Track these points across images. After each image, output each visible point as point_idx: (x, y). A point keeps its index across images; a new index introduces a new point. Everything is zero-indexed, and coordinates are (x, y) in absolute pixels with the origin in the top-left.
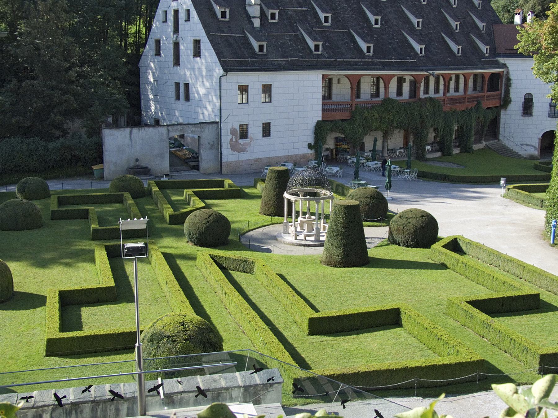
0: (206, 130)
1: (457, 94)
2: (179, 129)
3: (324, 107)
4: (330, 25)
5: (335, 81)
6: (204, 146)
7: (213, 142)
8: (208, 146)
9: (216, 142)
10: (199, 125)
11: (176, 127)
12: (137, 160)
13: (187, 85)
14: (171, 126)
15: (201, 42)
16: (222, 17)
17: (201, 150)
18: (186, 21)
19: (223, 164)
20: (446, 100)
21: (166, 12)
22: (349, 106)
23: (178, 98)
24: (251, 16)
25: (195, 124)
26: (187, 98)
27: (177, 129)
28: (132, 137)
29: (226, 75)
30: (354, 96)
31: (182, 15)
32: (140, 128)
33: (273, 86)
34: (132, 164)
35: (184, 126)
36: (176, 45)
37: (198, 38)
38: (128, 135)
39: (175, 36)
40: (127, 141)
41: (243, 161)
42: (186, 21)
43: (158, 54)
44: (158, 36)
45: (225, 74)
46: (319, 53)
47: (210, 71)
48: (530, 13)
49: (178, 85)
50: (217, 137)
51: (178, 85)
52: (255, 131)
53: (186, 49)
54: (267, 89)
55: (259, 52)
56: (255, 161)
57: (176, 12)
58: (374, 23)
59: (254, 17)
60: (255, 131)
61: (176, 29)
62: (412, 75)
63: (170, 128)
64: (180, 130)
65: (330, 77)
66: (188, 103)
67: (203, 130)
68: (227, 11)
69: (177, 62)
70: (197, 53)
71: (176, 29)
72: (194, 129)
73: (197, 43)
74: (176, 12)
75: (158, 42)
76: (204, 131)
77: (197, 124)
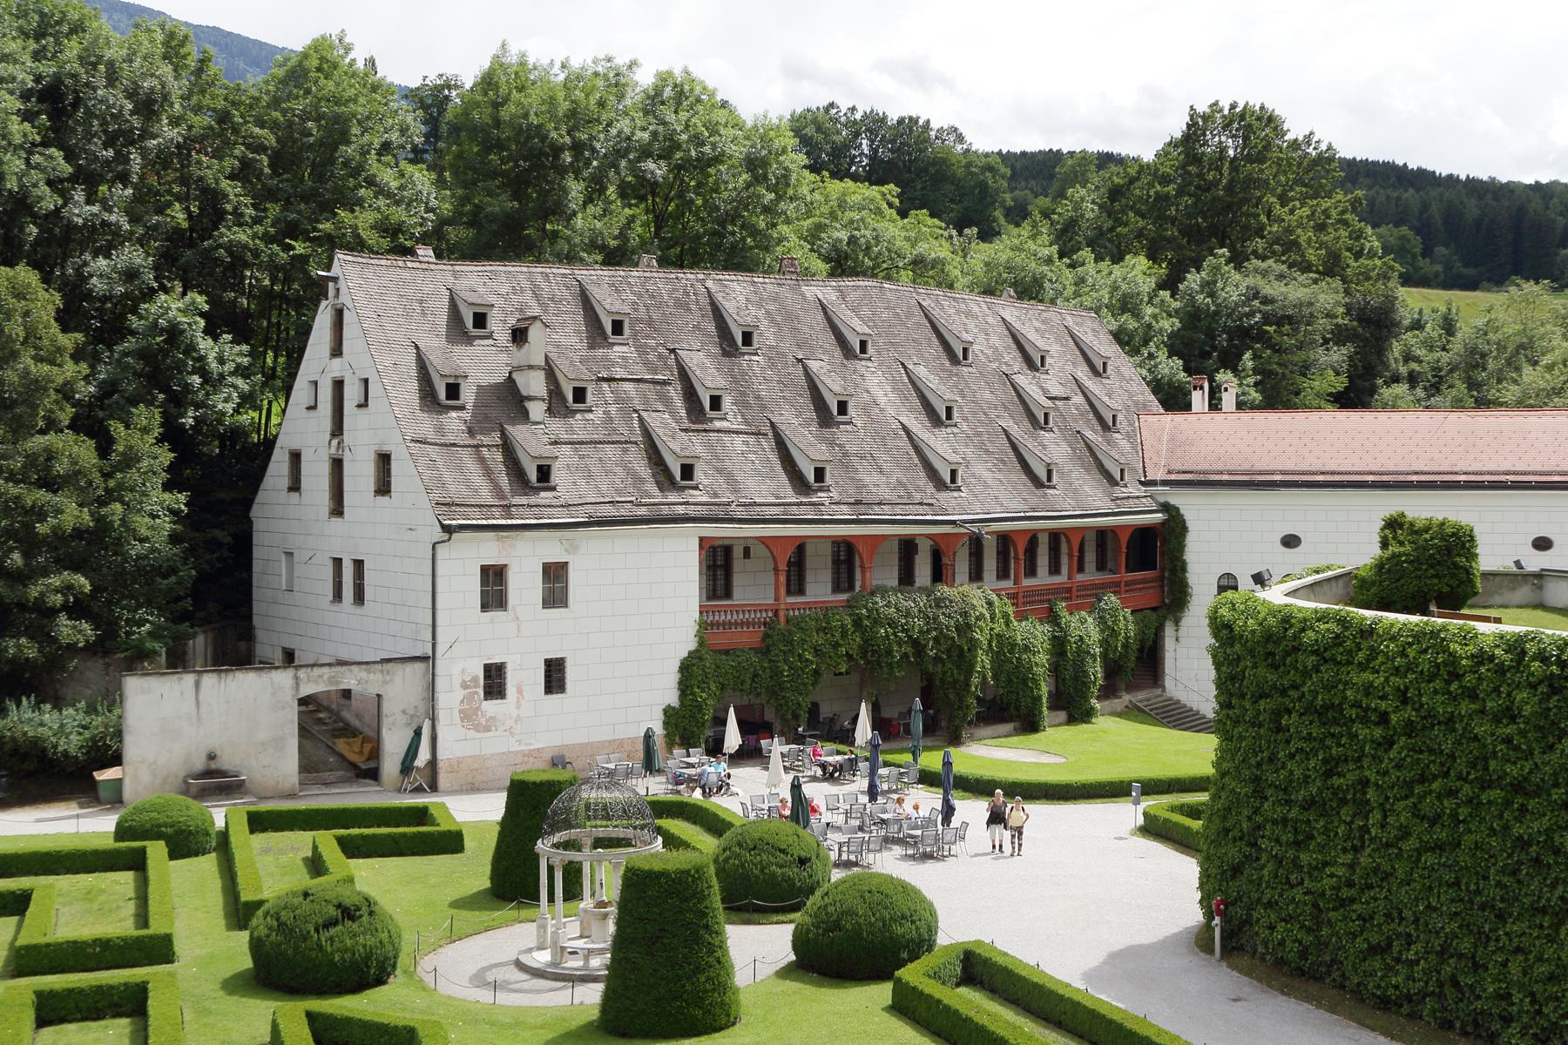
0: (398, 679)
1: (1057, 579)
2: (325, 677)
5: (738, 552)
6: (391, 720)
7: (416, 707)
9: (422, 709)
10: (379, 667)
11: (317, 671)
12: (212, 757)
13: (359, 564)
14: (304, 670)
15: (393, 457)
16: (447, 398)
18: (359, 406)
19: (440, 765)
20: (1021, 595)
21: (316, 383)
22: (770, 614)
23: (338, 596)
24: (524, 393)
25: (367, 663)
26: (359, 598)
27: (321, 676)
28: (201, 698)
30: (783, 591)
31: (352, 394)
32: (223, 675)
33: (571, 568)
34: (199, 764)
35: (339, 668)
36: (337, 464)
37: (386, 448)
38: (191, 692)
39: (335, 442)
40: (188, 705)
42: (359, 406)
43: (295, 486)
44: (295, 446)
45: (446, 536)
49: (338, 562)
50: (425, 695)
51: (338, 562)
52: (525, 677)
53: (360, 476)
54: (555, 576)
55: (539, 480)
56: (524, 756)
57: (339, 385)
58: (835, 413)
59: (530, 398)
60: (525, 677)
61: (338, 429)
62: (929, 536)
63: (302, 673)
64: (330, 677)
65: (727, 542)
66: (359, 610)
67: (388, 678)
69: (338, 510)
70: (383, 488)
71: (338, 429)
72: (364, 675)
73: (384, 459)
74: (339, 385)
75: (296, 457)
76: (391, 680)
77: (374, 663)
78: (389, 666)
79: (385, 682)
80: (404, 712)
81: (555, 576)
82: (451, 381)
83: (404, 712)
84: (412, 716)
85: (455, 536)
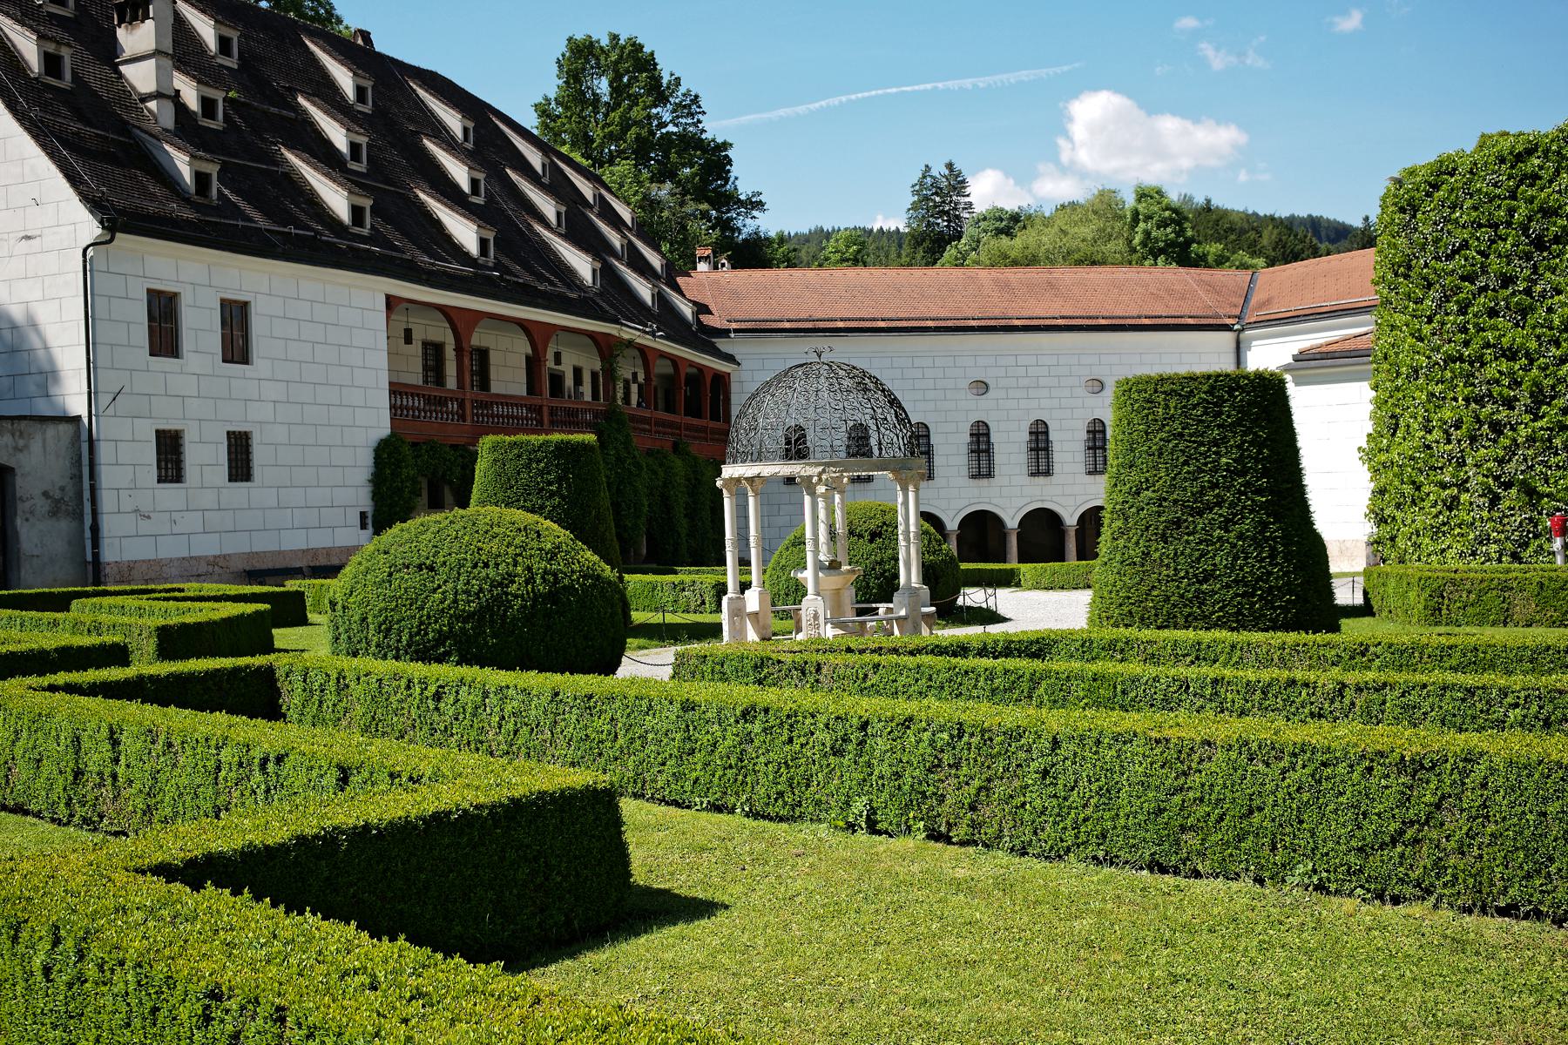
3: (393, 399)
4: (365, 171)
6: (27, 505)
7: (62, 489)
8: (42, 505)
9: (70, 492)
17: (19, 522)
19: (108, 570)
29: (111, 240)
41: (171, 560)
46: (365, 232)
47: (28, 238)
48: (724, 261)
54: (235, 317)
55: (197, 194)
67: (21, 443)
68: (66, 53)
76: (26, 447)
78: (24, 424)
79: (17, 449)
80: (46, 494)
81: (235, 317)
82: (51, 48)
83: (46, 494)
84: (57, 501)
85: (118, 235)
